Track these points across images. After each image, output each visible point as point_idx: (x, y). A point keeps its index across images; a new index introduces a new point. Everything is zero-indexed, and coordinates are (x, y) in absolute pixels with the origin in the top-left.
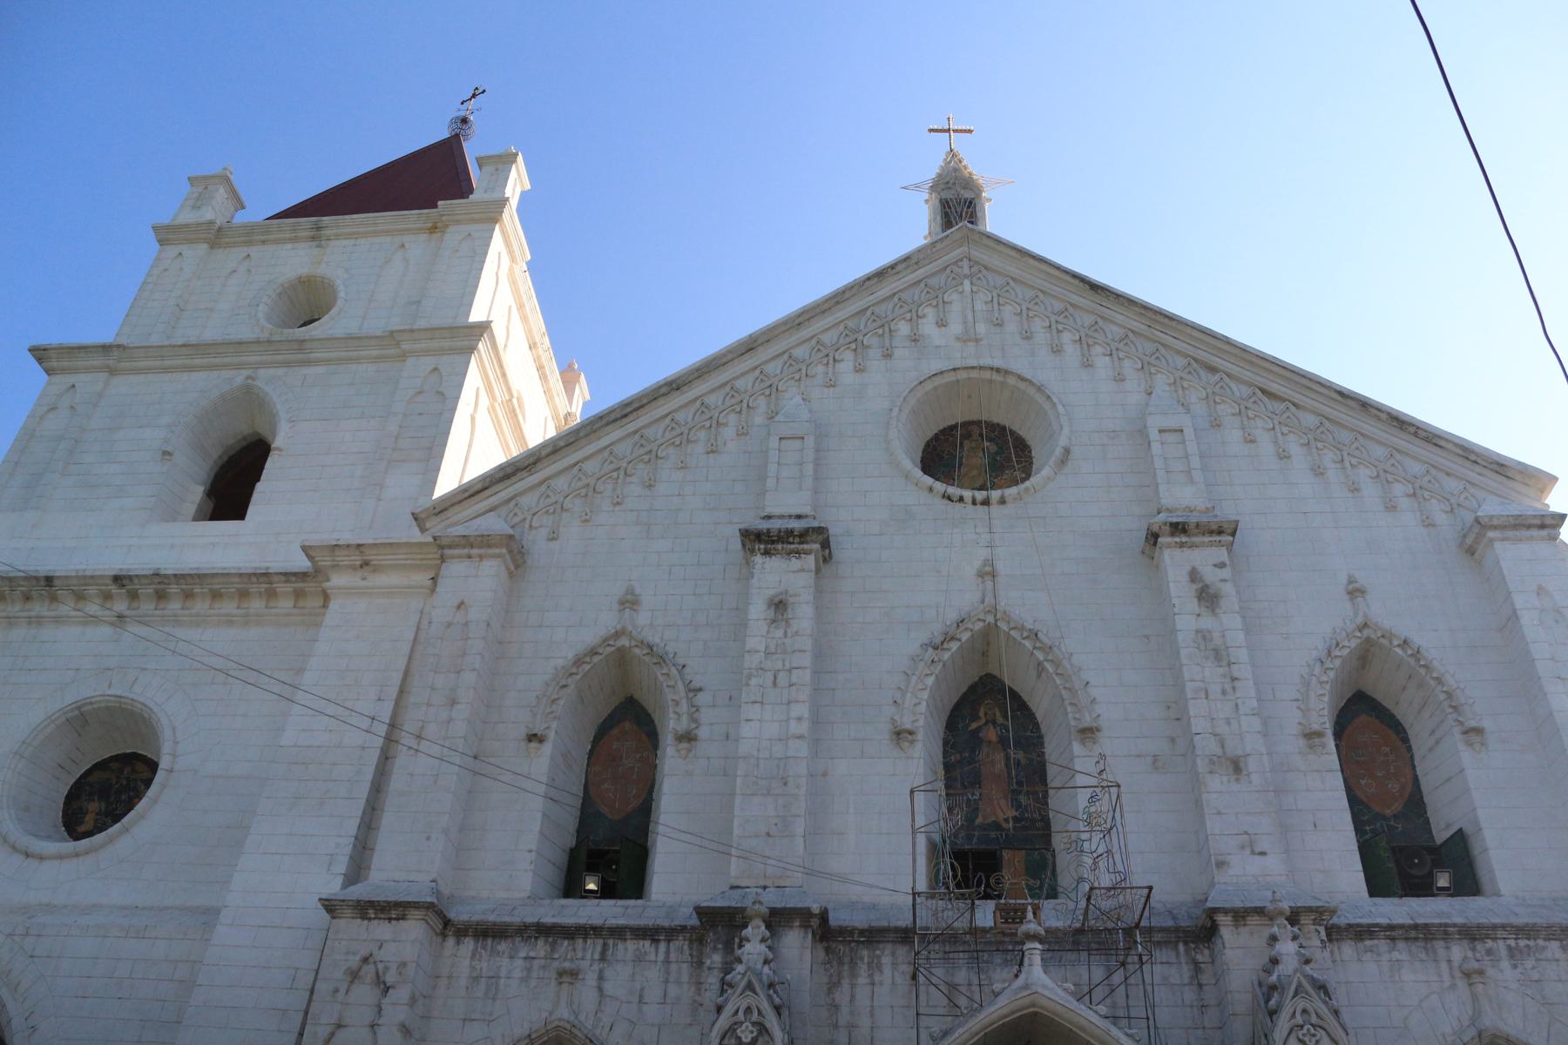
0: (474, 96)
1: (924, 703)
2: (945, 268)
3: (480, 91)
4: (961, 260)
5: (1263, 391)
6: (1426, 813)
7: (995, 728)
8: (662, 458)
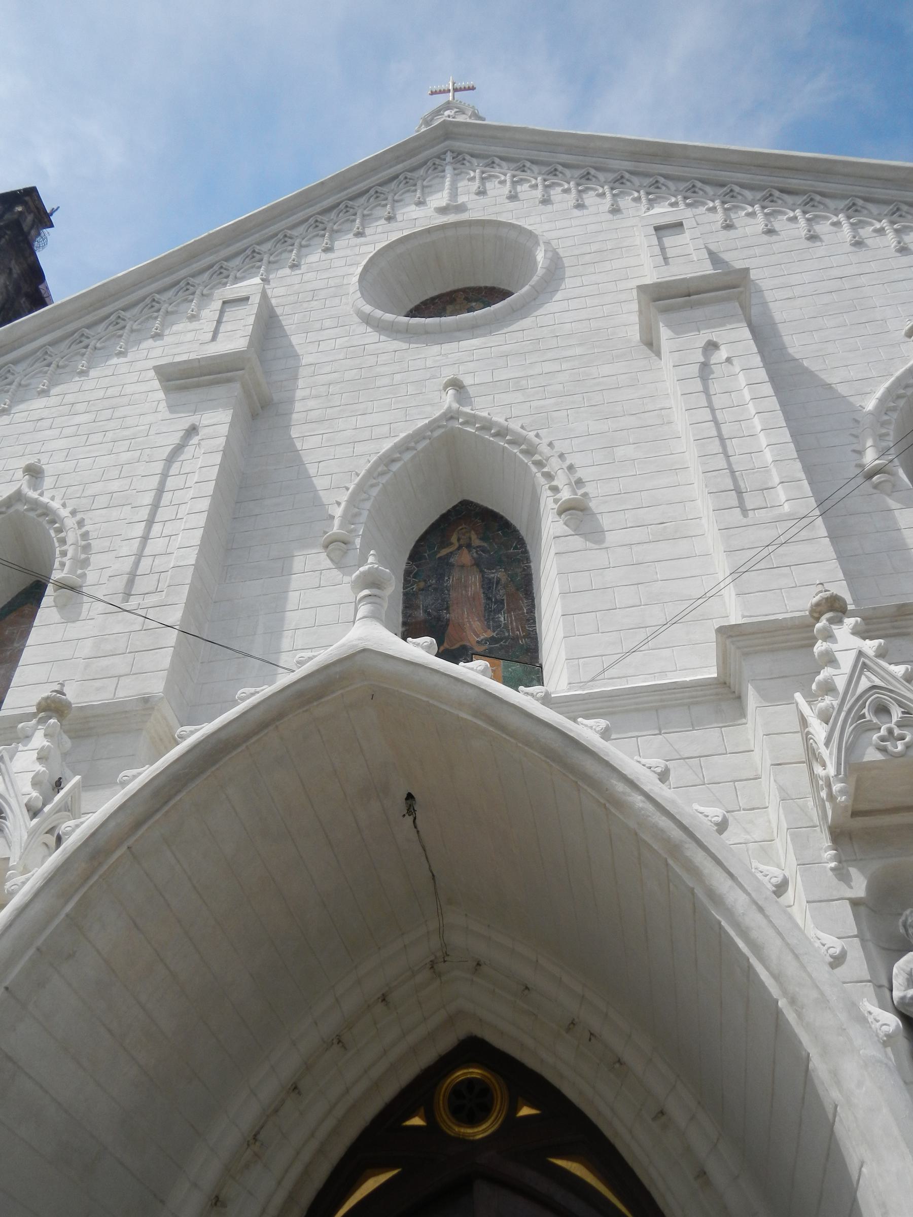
1: (365, 513)
4: (445, 153)
7: (469, 551)
8: (100, 349)
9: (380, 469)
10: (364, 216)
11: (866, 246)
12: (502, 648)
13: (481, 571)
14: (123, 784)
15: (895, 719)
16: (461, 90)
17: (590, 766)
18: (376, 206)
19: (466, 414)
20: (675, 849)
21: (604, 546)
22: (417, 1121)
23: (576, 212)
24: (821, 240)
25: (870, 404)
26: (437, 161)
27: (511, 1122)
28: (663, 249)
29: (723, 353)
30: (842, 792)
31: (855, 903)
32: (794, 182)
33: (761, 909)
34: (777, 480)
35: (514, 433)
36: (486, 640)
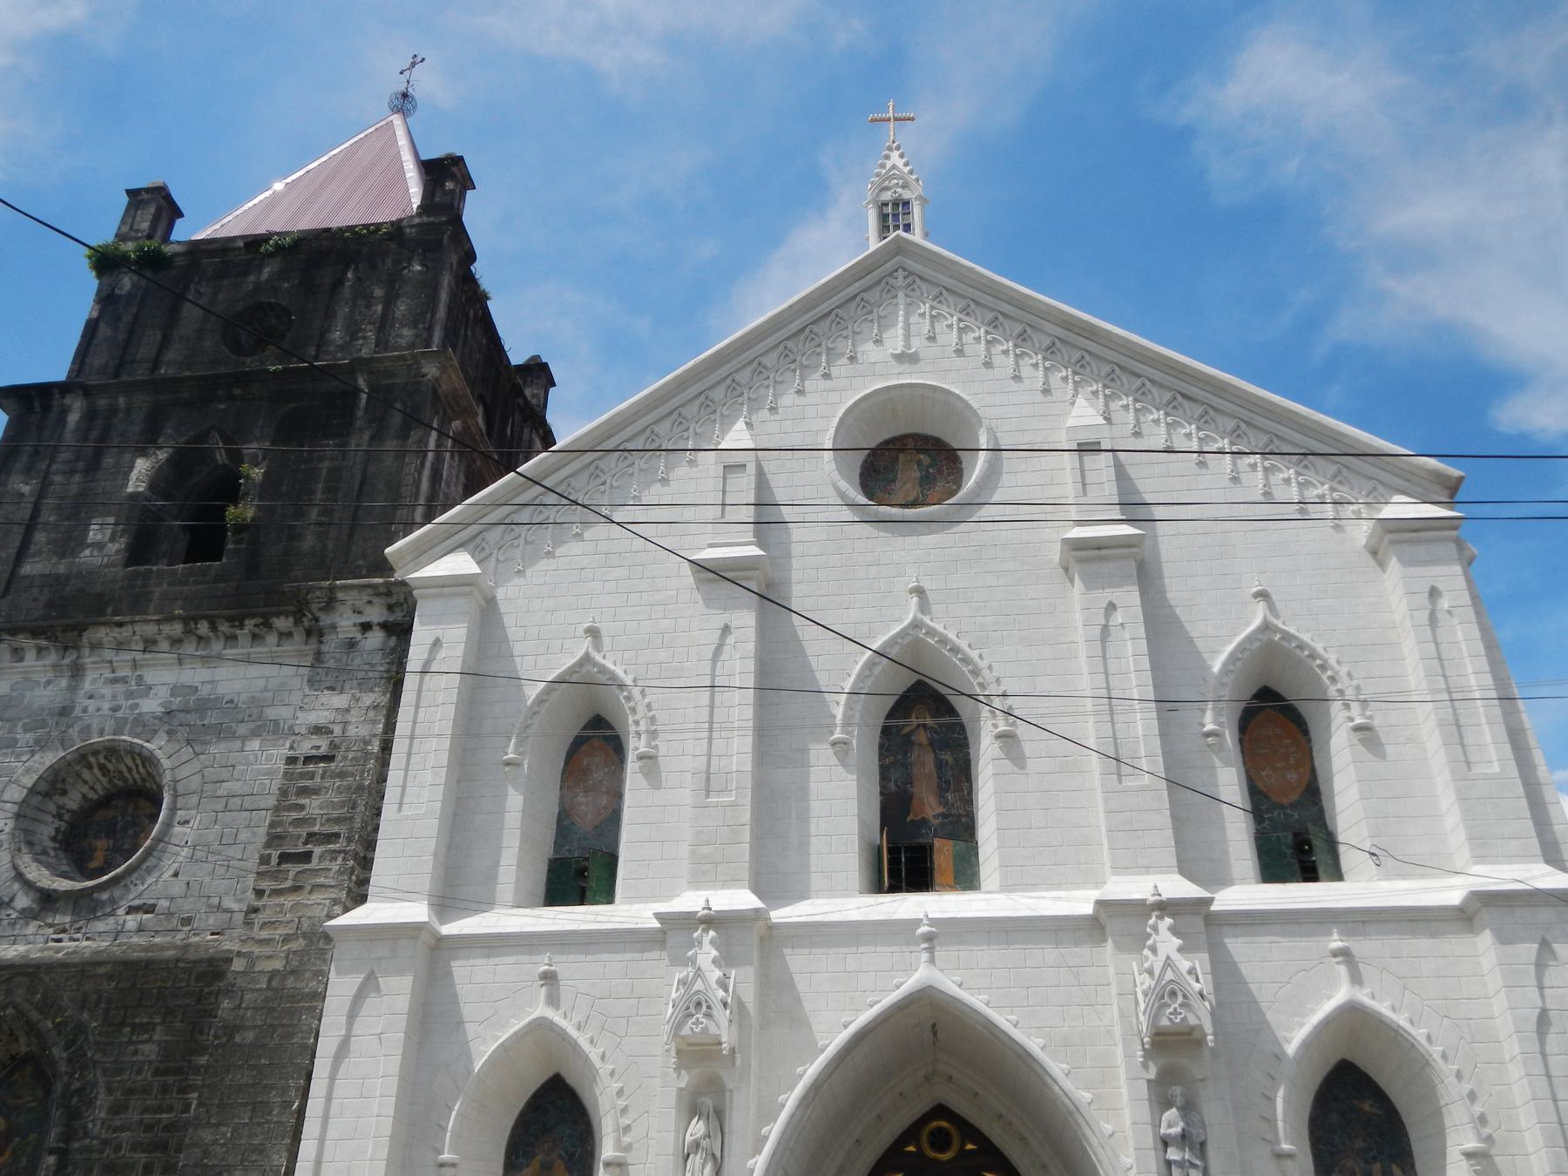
0: (413, 64)
1: (858, 715)
2: (880, 281)
3: (419, 59)
4: (896, 271)
5: (1184, 396)
6: (1320, 800)
7: (925, 731)
8: (616, 488)
9: (866, 673)
10: (828, 349)
11: (1240, 483)
12: (950, 823)
13: (934, 752)
14: (822, 1050)
15: (1179, 1002)
16: (900, 119)
18: (838, 337)
19: (929, 627)
20: (1071, 1114)
21: (1026, 771)
22: (911, 1148)
23: (1013, 386)
24: (1207, 468)
25: (1216, 667)
26: (891, 281)
27: (963, 1153)
28: (1082, 471)
29: (1118, 617)
30: (1148, 1043)
31: (1149, 1081)
32: (1194, 391)
33: (1103, 1148)
34: (1143, 754)
35: (964, 653)
36: (939, 815)
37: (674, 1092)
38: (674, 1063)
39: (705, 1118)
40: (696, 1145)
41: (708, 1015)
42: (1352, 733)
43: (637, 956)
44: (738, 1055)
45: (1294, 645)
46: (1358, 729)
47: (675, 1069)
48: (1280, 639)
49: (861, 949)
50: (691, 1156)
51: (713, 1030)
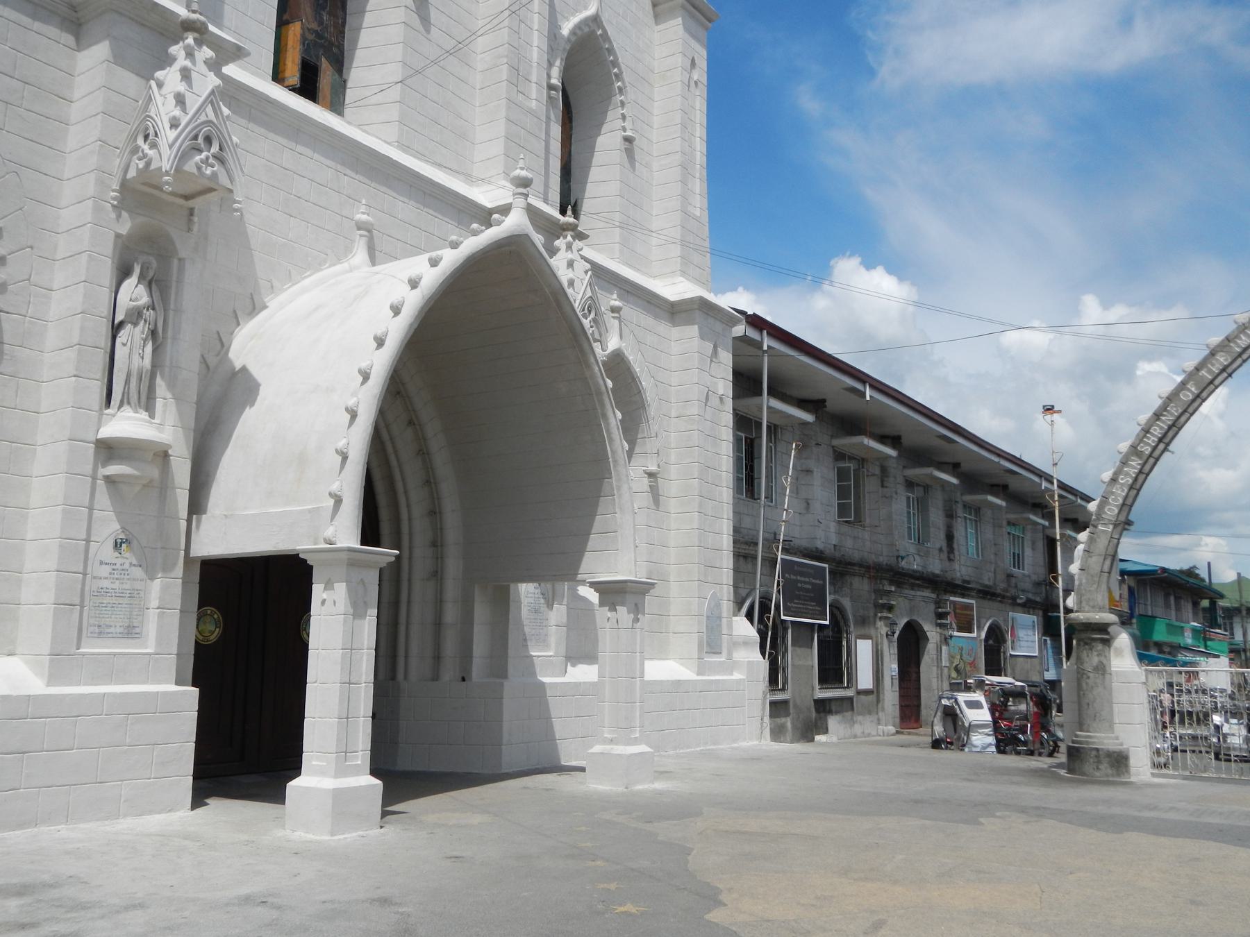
17: (586, 345)
37: (112, 236)
38: (114, 199)
39: (146, 283)
40: (135, 315)
41: (220, 159)
42: (623, 142)
43: (26, 20)
44: (196, 219)
45: (607, 46)
46: (628, 140)
47: (113, 206)
48: (600, 35)
49: (300, 148)
50: (129, 327)
51: (224, 180)
